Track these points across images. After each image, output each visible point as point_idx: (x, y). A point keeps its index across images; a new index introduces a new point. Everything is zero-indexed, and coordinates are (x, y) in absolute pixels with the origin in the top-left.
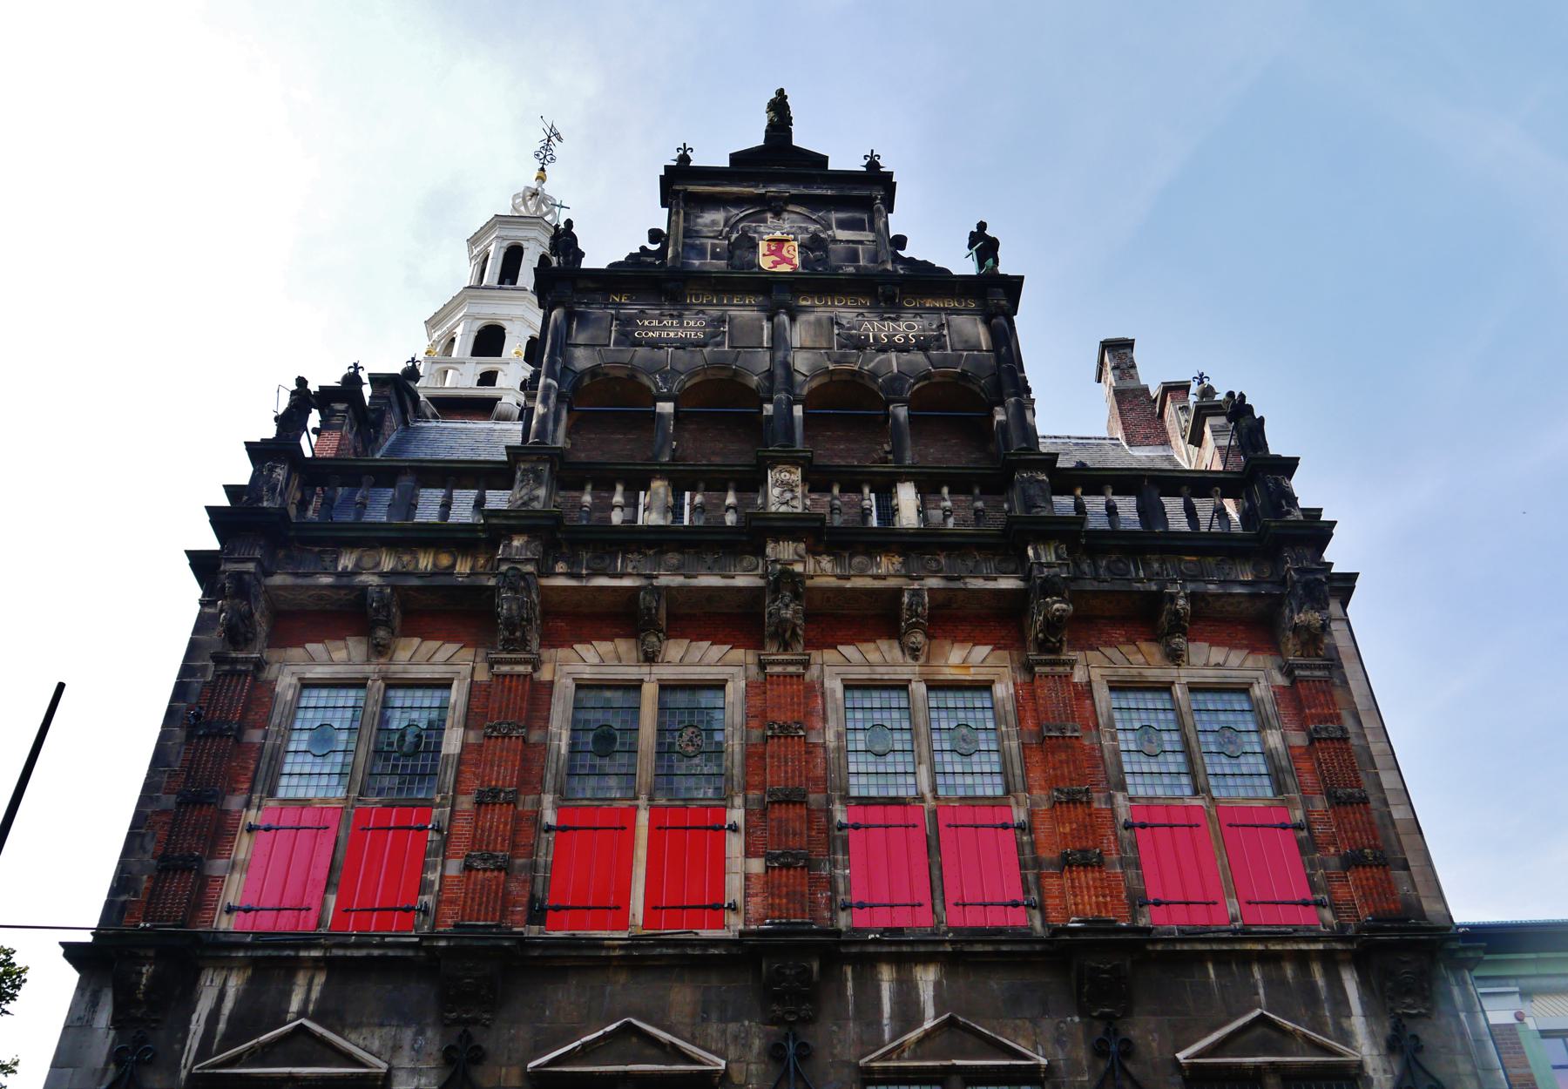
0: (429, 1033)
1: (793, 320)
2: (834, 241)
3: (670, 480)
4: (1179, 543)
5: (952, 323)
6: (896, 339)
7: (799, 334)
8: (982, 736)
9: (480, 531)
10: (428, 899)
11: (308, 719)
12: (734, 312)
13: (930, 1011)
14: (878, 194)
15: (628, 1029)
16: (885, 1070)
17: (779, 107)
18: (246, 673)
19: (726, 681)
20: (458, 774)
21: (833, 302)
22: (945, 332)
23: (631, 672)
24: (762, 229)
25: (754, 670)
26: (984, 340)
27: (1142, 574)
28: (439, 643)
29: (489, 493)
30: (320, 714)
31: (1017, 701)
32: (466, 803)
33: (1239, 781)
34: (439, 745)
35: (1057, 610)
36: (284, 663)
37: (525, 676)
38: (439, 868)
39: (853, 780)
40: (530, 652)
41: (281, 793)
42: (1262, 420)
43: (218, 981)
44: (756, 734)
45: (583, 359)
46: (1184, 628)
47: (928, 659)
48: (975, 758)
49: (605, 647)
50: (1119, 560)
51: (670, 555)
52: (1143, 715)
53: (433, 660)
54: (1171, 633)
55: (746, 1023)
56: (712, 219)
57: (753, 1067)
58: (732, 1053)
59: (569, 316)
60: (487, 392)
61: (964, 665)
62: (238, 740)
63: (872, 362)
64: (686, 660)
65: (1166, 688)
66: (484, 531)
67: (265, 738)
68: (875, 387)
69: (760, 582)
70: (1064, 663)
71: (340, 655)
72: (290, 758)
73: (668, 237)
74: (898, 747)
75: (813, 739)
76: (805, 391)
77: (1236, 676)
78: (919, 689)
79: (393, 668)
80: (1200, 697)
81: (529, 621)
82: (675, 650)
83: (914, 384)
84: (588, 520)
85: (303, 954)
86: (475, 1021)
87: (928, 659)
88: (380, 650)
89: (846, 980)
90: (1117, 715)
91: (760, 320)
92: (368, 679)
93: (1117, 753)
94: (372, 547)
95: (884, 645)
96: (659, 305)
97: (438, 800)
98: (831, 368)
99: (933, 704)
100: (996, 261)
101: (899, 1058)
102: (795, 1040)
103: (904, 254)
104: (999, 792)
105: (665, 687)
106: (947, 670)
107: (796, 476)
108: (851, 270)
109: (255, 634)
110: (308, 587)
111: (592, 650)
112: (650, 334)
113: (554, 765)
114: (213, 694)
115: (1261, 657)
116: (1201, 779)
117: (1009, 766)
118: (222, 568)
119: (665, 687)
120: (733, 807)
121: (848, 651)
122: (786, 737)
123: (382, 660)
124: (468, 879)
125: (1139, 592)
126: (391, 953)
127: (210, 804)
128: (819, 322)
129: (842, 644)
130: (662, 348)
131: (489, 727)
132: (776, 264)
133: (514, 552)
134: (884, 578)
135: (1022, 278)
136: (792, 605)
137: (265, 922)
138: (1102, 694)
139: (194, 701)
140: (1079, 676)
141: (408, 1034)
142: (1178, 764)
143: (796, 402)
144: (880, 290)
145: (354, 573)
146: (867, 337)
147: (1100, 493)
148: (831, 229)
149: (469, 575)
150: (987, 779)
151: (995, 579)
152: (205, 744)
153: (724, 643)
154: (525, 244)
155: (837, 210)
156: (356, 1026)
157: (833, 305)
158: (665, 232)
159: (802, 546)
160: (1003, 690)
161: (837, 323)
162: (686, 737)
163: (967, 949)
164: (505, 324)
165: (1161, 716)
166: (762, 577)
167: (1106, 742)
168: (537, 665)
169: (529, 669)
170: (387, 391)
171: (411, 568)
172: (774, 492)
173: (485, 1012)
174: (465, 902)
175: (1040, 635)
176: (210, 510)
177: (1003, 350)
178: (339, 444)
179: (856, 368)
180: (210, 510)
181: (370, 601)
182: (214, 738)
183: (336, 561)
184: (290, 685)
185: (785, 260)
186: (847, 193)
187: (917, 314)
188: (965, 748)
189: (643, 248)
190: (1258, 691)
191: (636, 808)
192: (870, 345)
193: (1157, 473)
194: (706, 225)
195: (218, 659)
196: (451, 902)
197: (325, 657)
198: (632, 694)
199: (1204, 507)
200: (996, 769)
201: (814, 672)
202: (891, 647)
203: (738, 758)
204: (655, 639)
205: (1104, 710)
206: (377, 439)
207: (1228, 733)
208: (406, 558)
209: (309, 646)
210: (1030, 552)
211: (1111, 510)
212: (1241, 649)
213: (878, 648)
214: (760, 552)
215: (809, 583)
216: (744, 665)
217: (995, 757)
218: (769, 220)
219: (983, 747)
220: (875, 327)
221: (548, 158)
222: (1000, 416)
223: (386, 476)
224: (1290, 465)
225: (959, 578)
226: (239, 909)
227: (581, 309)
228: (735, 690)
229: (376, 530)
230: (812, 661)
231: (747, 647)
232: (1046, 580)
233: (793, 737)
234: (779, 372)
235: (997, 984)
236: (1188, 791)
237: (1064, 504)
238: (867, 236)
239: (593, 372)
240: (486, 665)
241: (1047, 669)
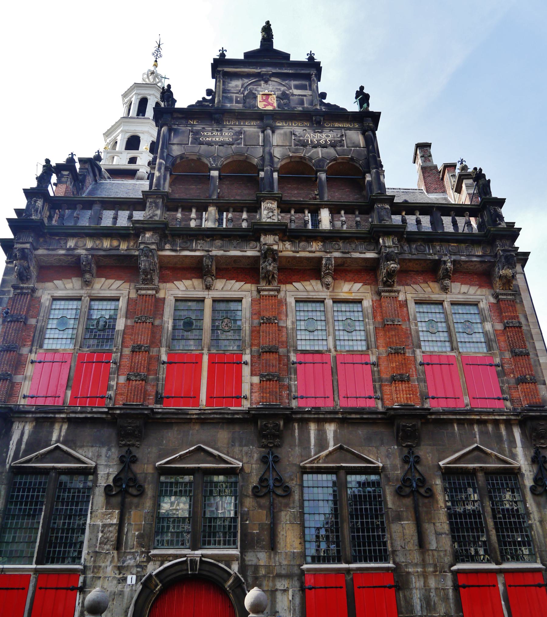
0: (113, 450)
1: (273, 132)
2: (293, 95)
3: (217, 207)
4: (449, 237)
5: (347, 134)
6: (321, 141)
7: (276, 139)
8: (357, 323)
10: (111, 393)
11: (56, 314)
12: (246, 129)
13: (331, 443)
14: (313, 72)
15: (200, 449)
16: (312, 468)
17: (267, 30)
18: (27, 294)
19: (243, 298)
20: (123, 338)
21: (292, 124)
22: (344, 138)
23: (200, 294)
24: (259, 89)
25: (255, 293)
26: (362, 142)
27: (431, 251)
28: (114, 280)
29: (134, 212)
30: (61, 312)
31: (373, 308)
32: (127, 351)
33: (472, 345)
34: (114, 325)
35: (393, 267)
36: (44, 289)
37: (152, 295)
38: (116, 380)
39: (299, 343)
40: (154, 285)
41: (45, 347)
42: (489, 181)
43: (21, 427)
44: (256, 322)
45: (176, 151)
46: (450, 276)
47: (333, 289)
48: (354, 333)
49: (188, 283)
50: (421, 245)
51: (217, 241)
52: (430, 315)
53: (111, 288)
54: (444, 278)
55: (251, 447)
56: (236, 84)
57: (254, 466)
58: (245, 459)
59: (170, 130)
60: (132, 167)
61: (350, 292)
62: (25, 323)
63: (310, 152)
64: (225, 289)
65: (440, 303)
66: (133, 230)
67: (37, 322)
68: (311, 165)
69: (258, 254)
70: (395, 291)
71: (69, 286)
72: (48, 331)
73: (215, 93)
74: (319, 328)
75: (282, 324)
76: (279, 166)
77: (472, 298)
78: (329, 302)
79: (93, 292)
80: (456, 307)
81: (154, 270)
82: (219, 284)
83: (329, 163)
84: (180, 225)
85: (57, 416)
86: (133, 445)
87: (333, 289)
88: (87, 283)
89: (295, 429)
90: (418, 315)
91: (258, 132)
93: (417, 332)
94: (82, 237)
95: (313, 282)
96: (211, 125)
97: (115, 350)
98: (291, 155)
99: (335, 309)
100: (368, 105)
101: (318, 463)
102: (272, 455)
103: (325, 101)
104: (364, 348)
105: (215, 301)
106: (342, 294)
107: (274, 205)
108: (300, 109)
109: (31, 276)
110: (54, 255)
111: (182, 284)
112: (207, 139)
113: (166, 335)
114: (13, 303)
115: (484, 290)
116: (455, 344)
117: (369, 337)
118: (15, 246)
119: (215, 301)
120: (245, 354)
121: (298, 285)
122: (269, 323)
123: (88, 288)
124: (129, 384)
125: (430, 260)
126: (95, 416)
127: (14, 351)
128: (285, 134)
129: (294, 282)
130: (213, 145)
131: (136, 318)
132: (265, 106)
133: (146, 239)
134: (314, 252)
135: (380, 113)
136: (272, 264)
137: (40, 402)
138: (411, 305)
139: (5, 306)
140: (401, 297)
141: (104, 450)
142: (445, 337)
143: (275, 171)
144: (314, 118)
145: (74, 249)
146: (308, 141)
147: (414, 214)
148: (291, 89)
149: (126, 250)
150: (359, 343)
151: (365, 253)
152: (11, 325)
153: (242, 281)
154: (148, 97)
155: (294, 80)
156: (82, 447)
157: (292, 126)
158: (214, 90)
159: (277, 237)
160: (367, 303)
161: (294, 134)
162: (224, 324)
163: (349, 416)
164: (140, 135)
165: (438, 315)
166: (259, 251)
167: (413, 327)
168: (157, 290)
169: (154, 292)
170: (87, 166)
171: (100, 247)
172: (264, 213)
173: (137, 441)
174: (127, 394)
175: (385, 279)
176: (9, 220)
177: (371, 147)
178: (66, 191)
179: (302, 155)
180: (9, 220)
181: (82, 261)
182: (15, 322)
183: (66, 243)
184: (47, 299)
185: (269, 104)
186: (299, 72)
187: (331, 130)
188: (349, 329)
189: (204, 98)
190: (482, 305)
191: (202, 354)
192: (309, 145)
193: (440, 205)
194: (233, 87)
195: (15, 287)
196: (121, 394)
197: (63, 286)
198: (201, 304)
199: (461, 221)
200: (363, 338)
201: (282, 294)
202: (317, 283)
203: (248, 332)
204: (210, 279)
205: (412, 313)
206: (83, 188)
207: (467, 324)
208: (98, 242)
209: (55, 282)
210: (381, 241)
211: (418, 222)
212: (475, 286)
213: (311, 284)
214: (258, 240)
215: (280, 254)
216: (251, 291)
217: (363, 333)
218: (262, 85)
219: (358, 328)
220: (311, 136)
221: (159, 55)
222: (368, 178)
223: (88, 204)
224: (501, 202)
225: (348, 253)
226: (28, 397)
227: (175, 127)
228: (247, 302)
229: (84, 229)
230: (281, 290)
231: (252, 283)
232: (388, 254)
233: (272, 323)
234: (267, 157)
235: (361, 432)
236: (449, 349)
237: (397, 219)
238: (308, 92)
239: (181, 157)
240: (135, 290)
241: (387, 294)
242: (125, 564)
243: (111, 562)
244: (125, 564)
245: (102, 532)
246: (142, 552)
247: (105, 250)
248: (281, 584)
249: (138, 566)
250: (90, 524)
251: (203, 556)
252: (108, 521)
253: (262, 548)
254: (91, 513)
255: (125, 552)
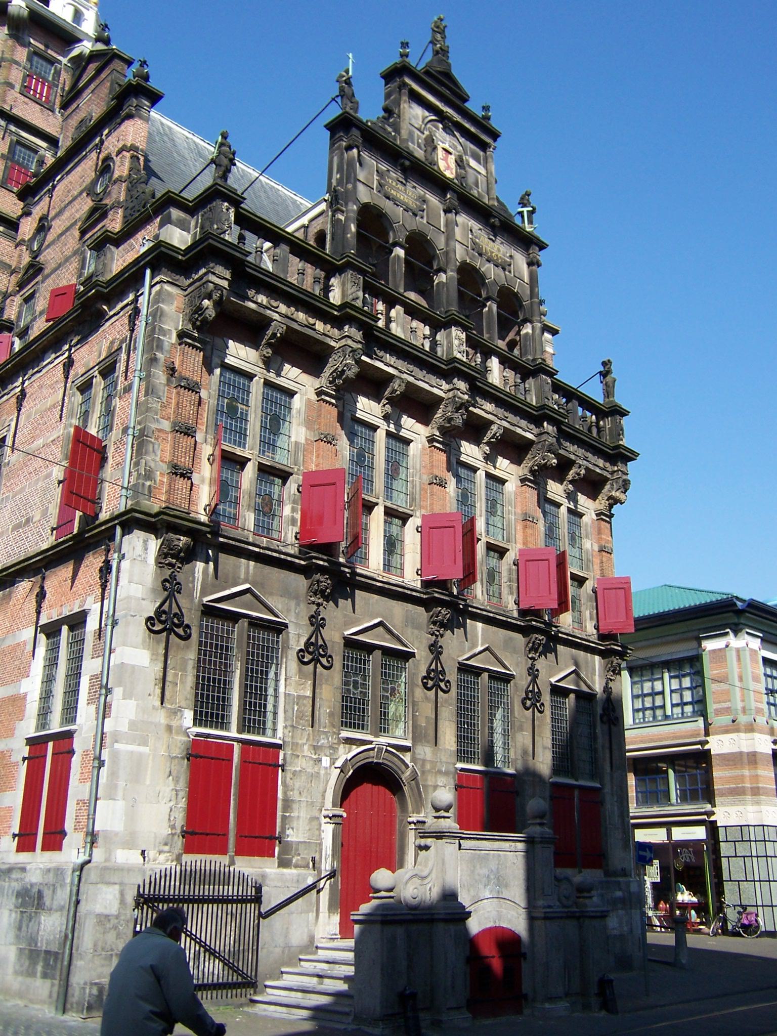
9: (336, 310)
92: (256, 375)
134: (487, 412)
175: (536, 468)
186: (479, 135)
242: (319, 744)
243: (307, 740)
244: (319, 744)
245: (297, 704)
246: (334, 733)
247: (301, 325)
248: (441, 781)
249: (331, 747)
250: (285, 693)
252: (301, 693)
253: (428, 742)
254: (286, 680)
255: (319, 731)
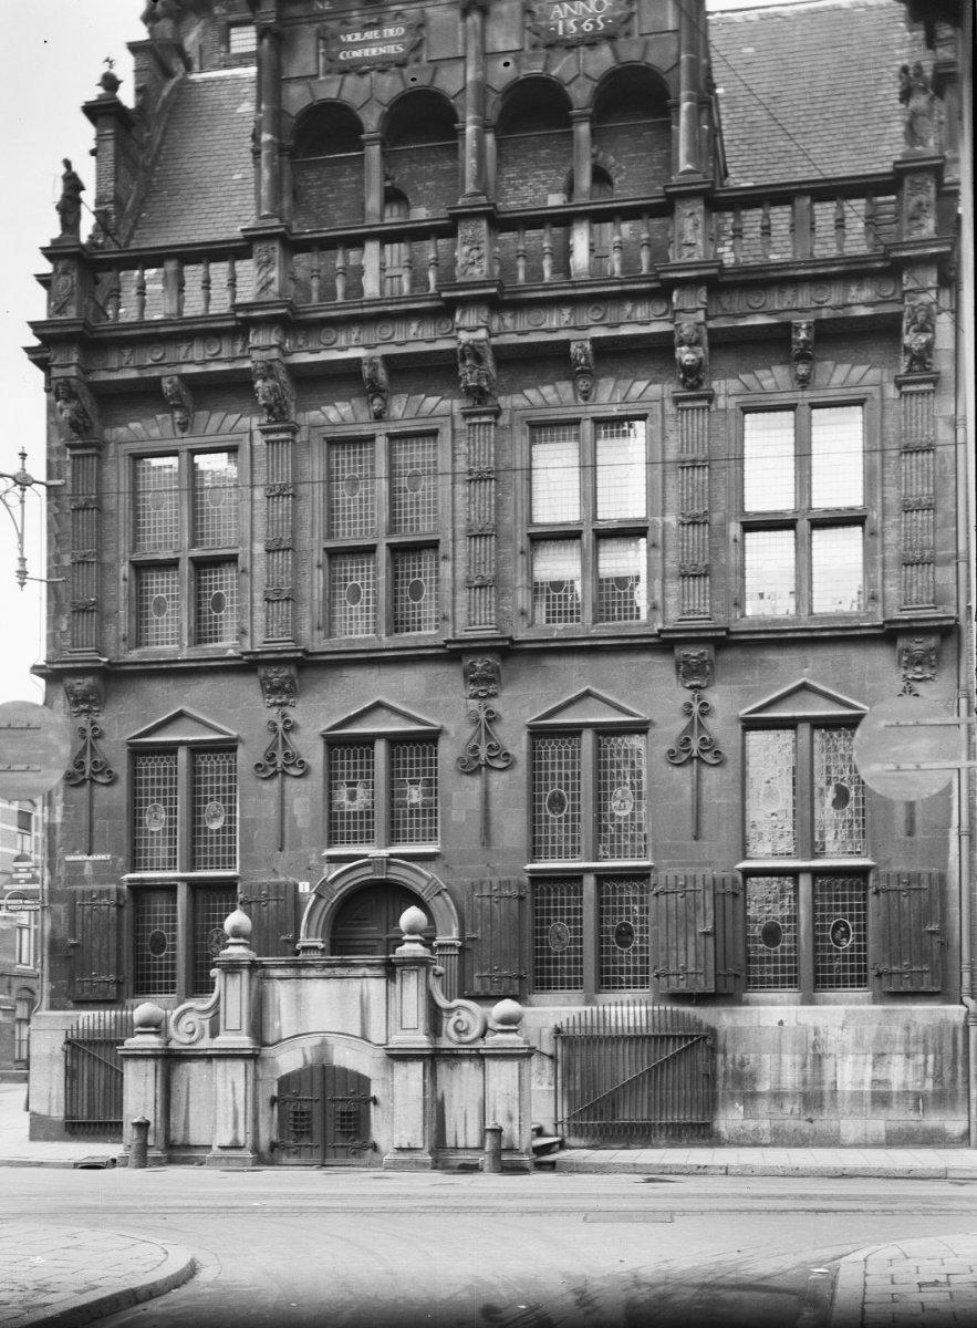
23: (366, 430)
82: (399, 407)
129: (528, 388)
134: (555, 331)
251: (392, 856)
